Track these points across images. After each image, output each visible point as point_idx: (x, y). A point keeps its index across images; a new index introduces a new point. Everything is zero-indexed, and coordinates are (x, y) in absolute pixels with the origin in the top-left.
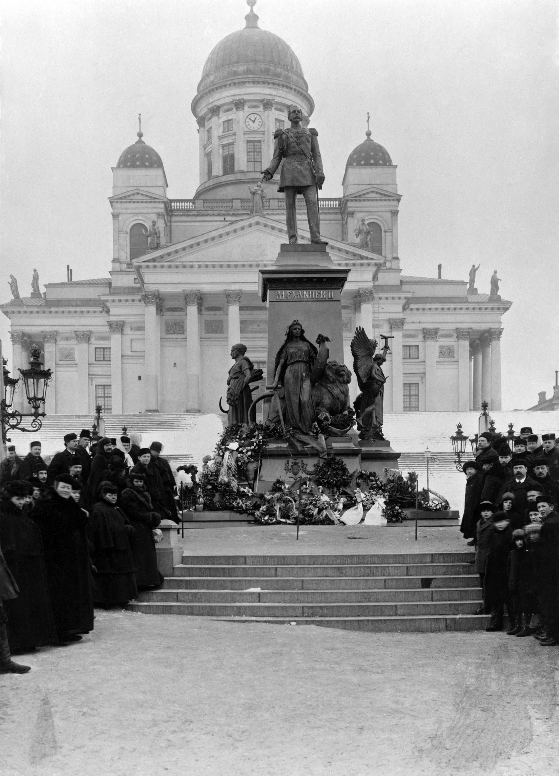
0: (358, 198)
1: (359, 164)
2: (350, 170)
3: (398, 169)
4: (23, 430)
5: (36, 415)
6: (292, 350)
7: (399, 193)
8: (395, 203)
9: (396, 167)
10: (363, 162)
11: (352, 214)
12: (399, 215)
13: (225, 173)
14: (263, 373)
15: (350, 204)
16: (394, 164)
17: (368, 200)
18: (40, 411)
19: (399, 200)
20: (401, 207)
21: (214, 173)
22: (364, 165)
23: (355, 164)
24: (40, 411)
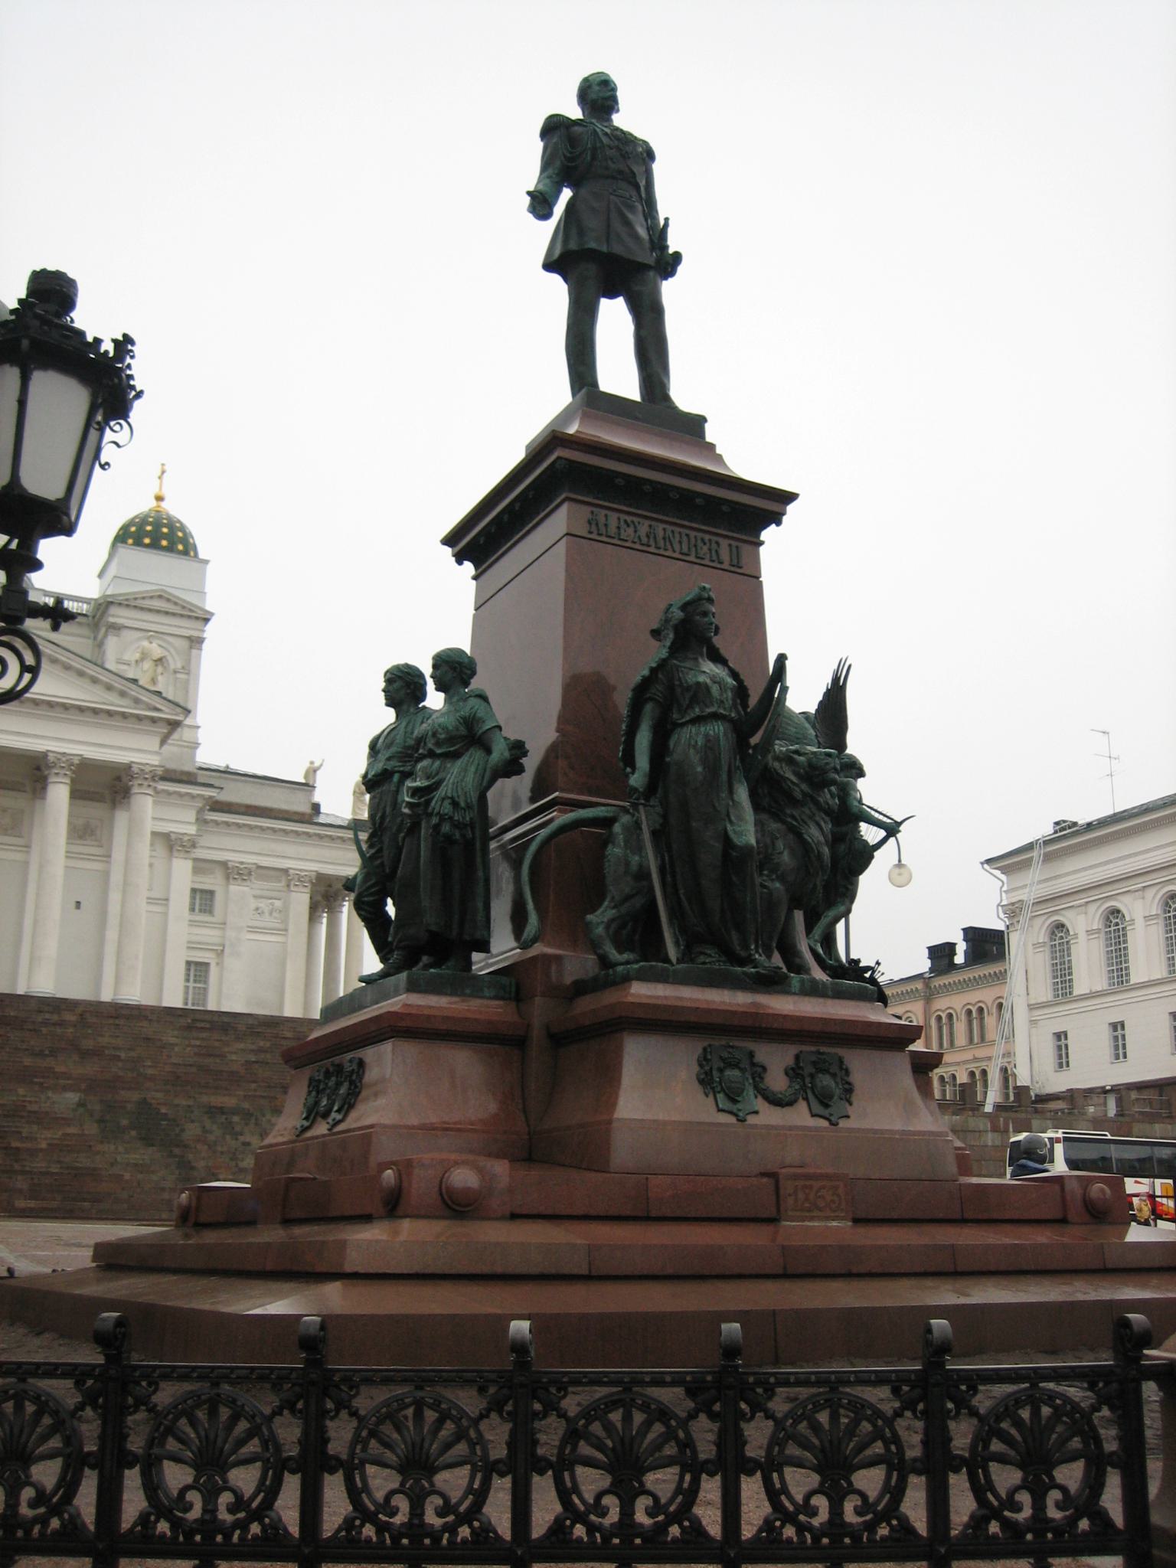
0: (128, 603)
1: (138, 543)
2: (123, 551)
3: (209, 567)
7: (208, 608)
8: (198, 624)
9: (206, 562)
10: (147, 541)
11: (116, 628)
12: (205, 646)
14: (525, 754)
15: (113, 610)
16: (201, 556)
17: (150, 610)
19: (207, 620)
20: (210, 631)
22: (147, 546)
23: (130, 541)
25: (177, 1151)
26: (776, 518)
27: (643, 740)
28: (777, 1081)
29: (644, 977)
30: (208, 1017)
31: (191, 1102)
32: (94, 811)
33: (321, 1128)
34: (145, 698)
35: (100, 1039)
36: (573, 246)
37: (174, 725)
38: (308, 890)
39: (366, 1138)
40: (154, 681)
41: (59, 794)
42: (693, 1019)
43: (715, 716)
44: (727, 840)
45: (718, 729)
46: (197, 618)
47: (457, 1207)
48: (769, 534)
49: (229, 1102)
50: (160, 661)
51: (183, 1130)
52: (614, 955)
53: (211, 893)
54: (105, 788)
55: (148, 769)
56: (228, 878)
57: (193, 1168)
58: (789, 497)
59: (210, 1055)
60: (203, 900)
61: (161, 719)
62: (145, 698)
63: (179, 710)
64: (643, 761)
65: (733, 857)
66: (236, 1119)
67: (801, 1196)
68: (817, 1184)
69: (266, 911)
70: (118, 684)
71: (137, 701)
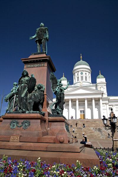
28: (20, 124)
32: (97, 102)
37: (103, 93)
42: (10, 117)
43: (23, 83)
67: (13, 138)
68: (15, 137)
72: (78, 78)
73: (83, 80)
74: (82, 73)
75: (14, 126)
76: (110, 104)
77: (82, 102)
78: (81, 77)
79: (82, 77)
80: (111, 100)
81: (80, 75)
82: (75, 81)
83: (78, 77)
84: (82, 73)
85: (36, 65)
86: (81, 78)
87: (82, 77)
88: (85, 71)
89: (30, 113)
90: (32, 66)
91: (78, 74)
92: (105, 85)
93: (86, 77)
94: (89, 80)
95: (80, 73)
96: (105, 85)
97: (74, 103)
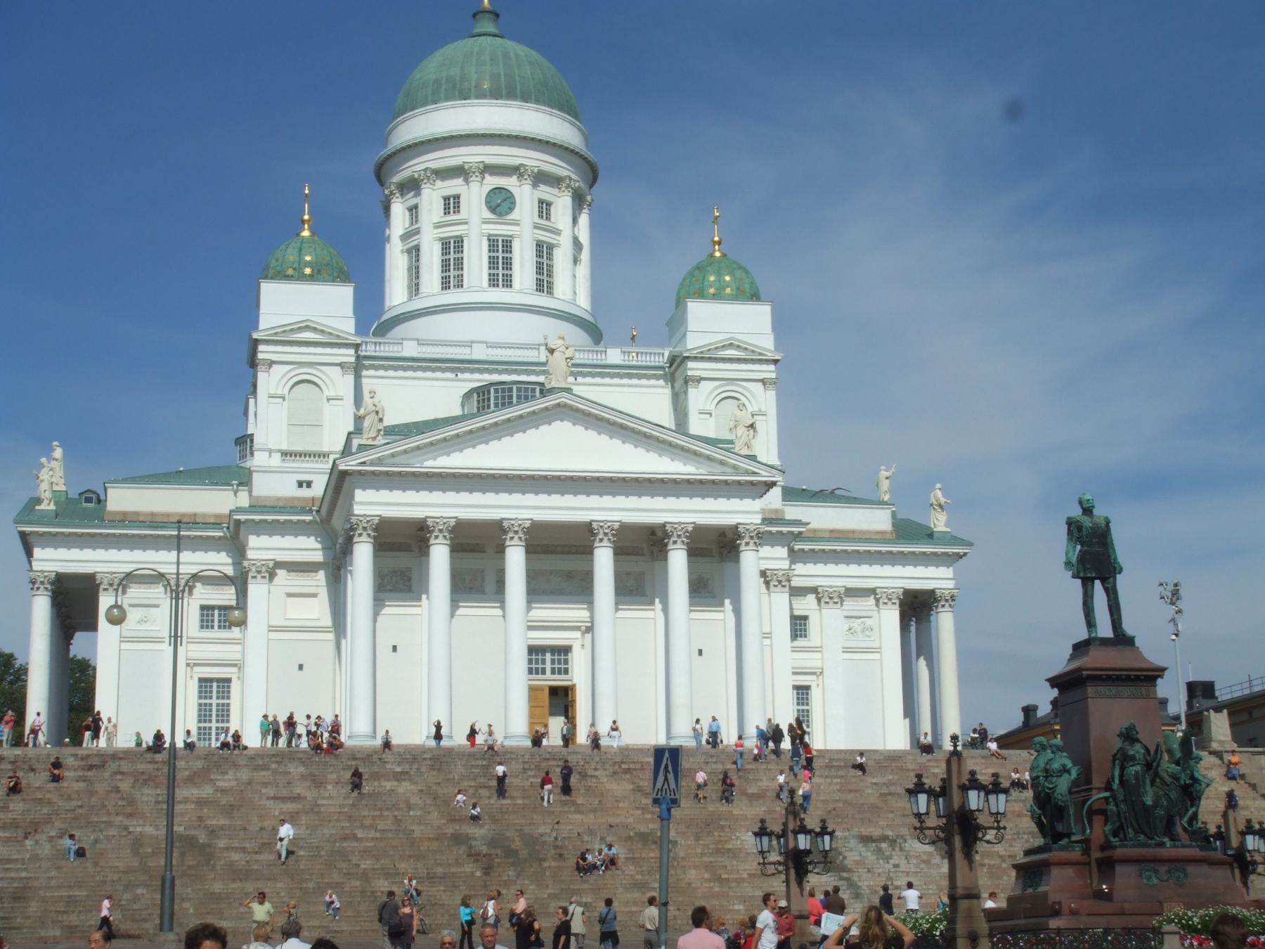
4: (988, 842)
5: (998, 828)
6: (1131, 752)
10: (712, 291)
13: (445, 285)
18: (1001, 824)
21: (424, 289)
24: (1001, 824)
25: (845, 875)
26: (1161, 677)
27: (1117, 773)
29: (1121, 846)
30: (841, 756)
31: (846, 834)
33: (1030, 890)
34: (745, 465)
35: (760, 784)
36: (1082, 575)
38: (897, 607)
39: (1045, 894)
40: (748, 445)
41: (678, 561)
44: (1144, 804)
45: (1138, 768)
46: (768, 361)
47: (1074, 913)
48: (1159, 681)
49: (876, 832)
50: (752, 426)
51: (845, 858)
52: (1112, 839)
53: (806, 618)
54: (716, 550)
55: (752, 528)
56: (819, 600)
57: (859, 887)
58: (1163, 670)
59: (851, 791)
60: (799, 626)
61: (760, 482)
62: (745, 465)
63: (774, 472)
64: (1117, 781)
65: (1146, 809)
66: (884, 845)
69: (859, 629)
70: (717, 454)
71: (735, 467)
72: (453, 248)
73: (508, 282)
74: (500, 203)
75: (1149, 878)
76: (807, 573)
77: (560, 559)
78: (493, 243)
79: (500, 253)
80: (816, 536)
81: (476, 224)
82: (414, 287)
83: (459, 242)
84: (500, 203)
85: (1126, 690)
86: (493, 263)
87: (500, 253)
88: (541, 178)
89: (1174, 846)
90: (1113, 690)
91: (452, 204)
92: (763, 381)
93: (544, 251)
94: (574, 286)
95: (474, 195)
96: (763, 381)
97: (471, 562)
